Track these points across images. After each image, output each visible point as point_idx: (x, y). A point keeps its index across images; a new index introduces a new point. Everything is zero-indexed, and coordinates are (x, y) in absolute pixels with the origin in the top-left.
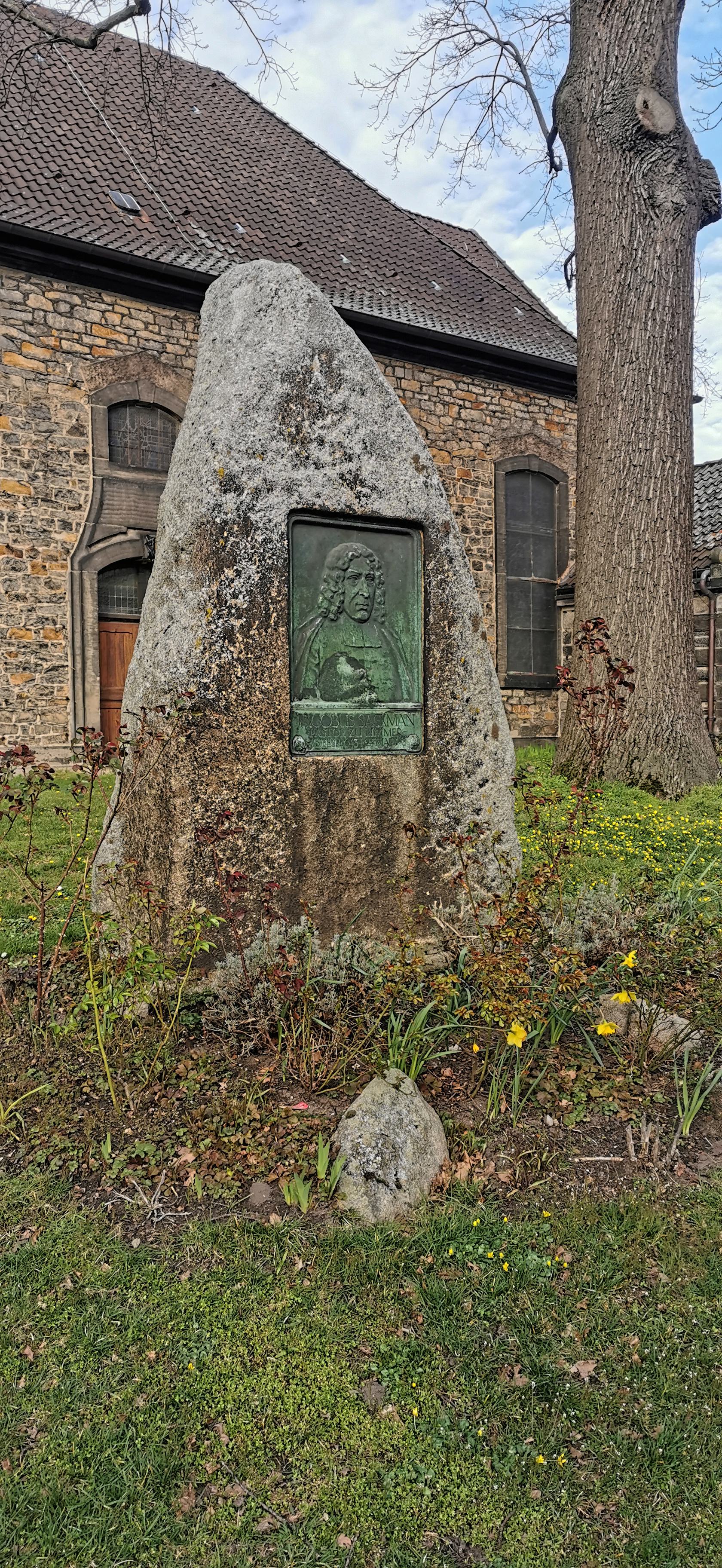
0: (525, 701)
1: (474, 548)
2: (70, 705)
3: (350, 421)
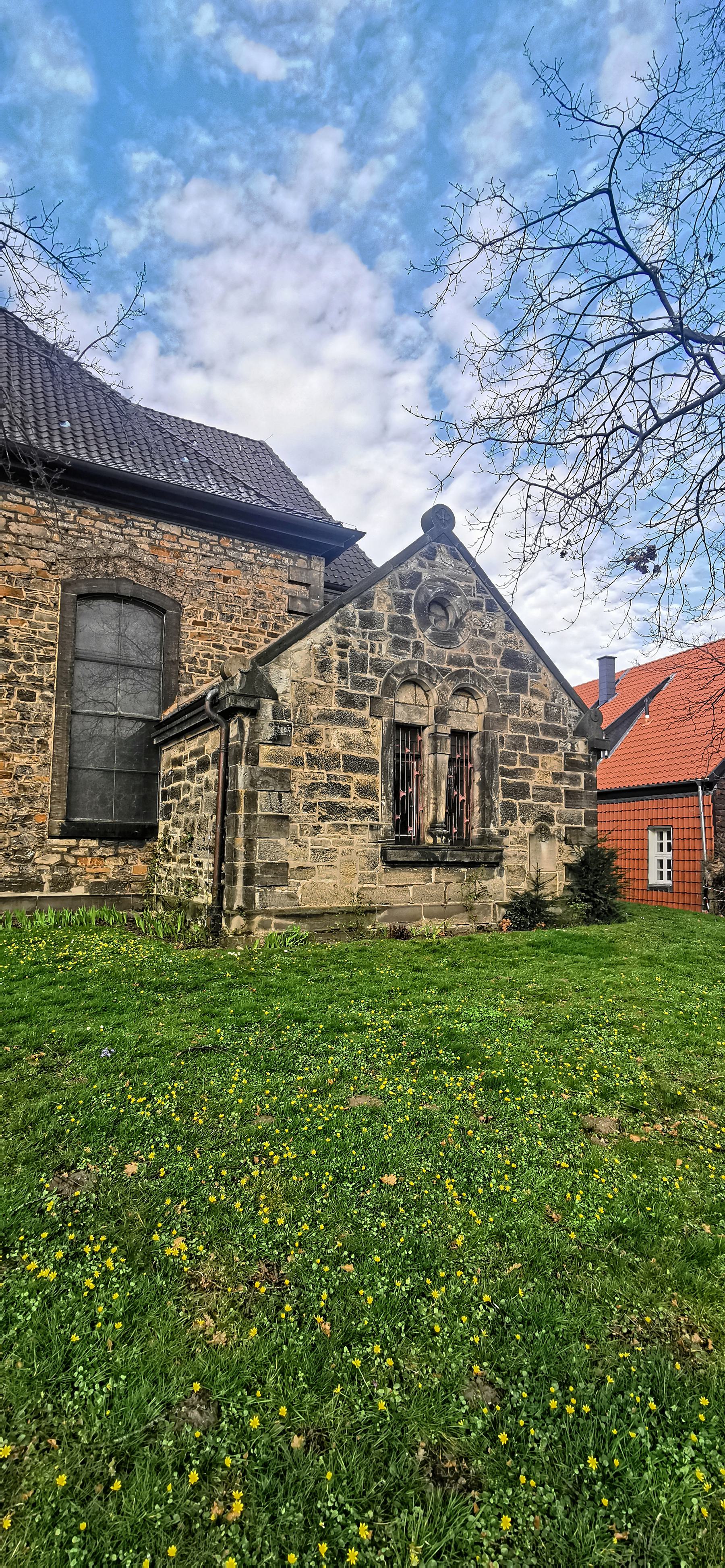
0: (99, 852)
1: (23, 676)
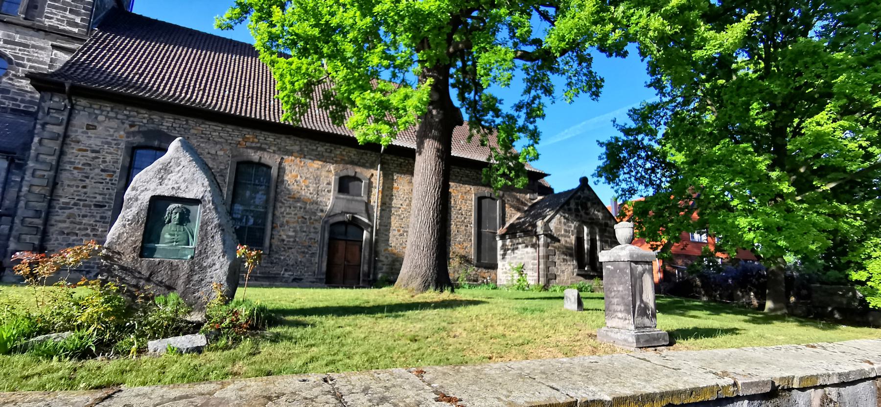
2: (317, 265)
3: (180, 174)
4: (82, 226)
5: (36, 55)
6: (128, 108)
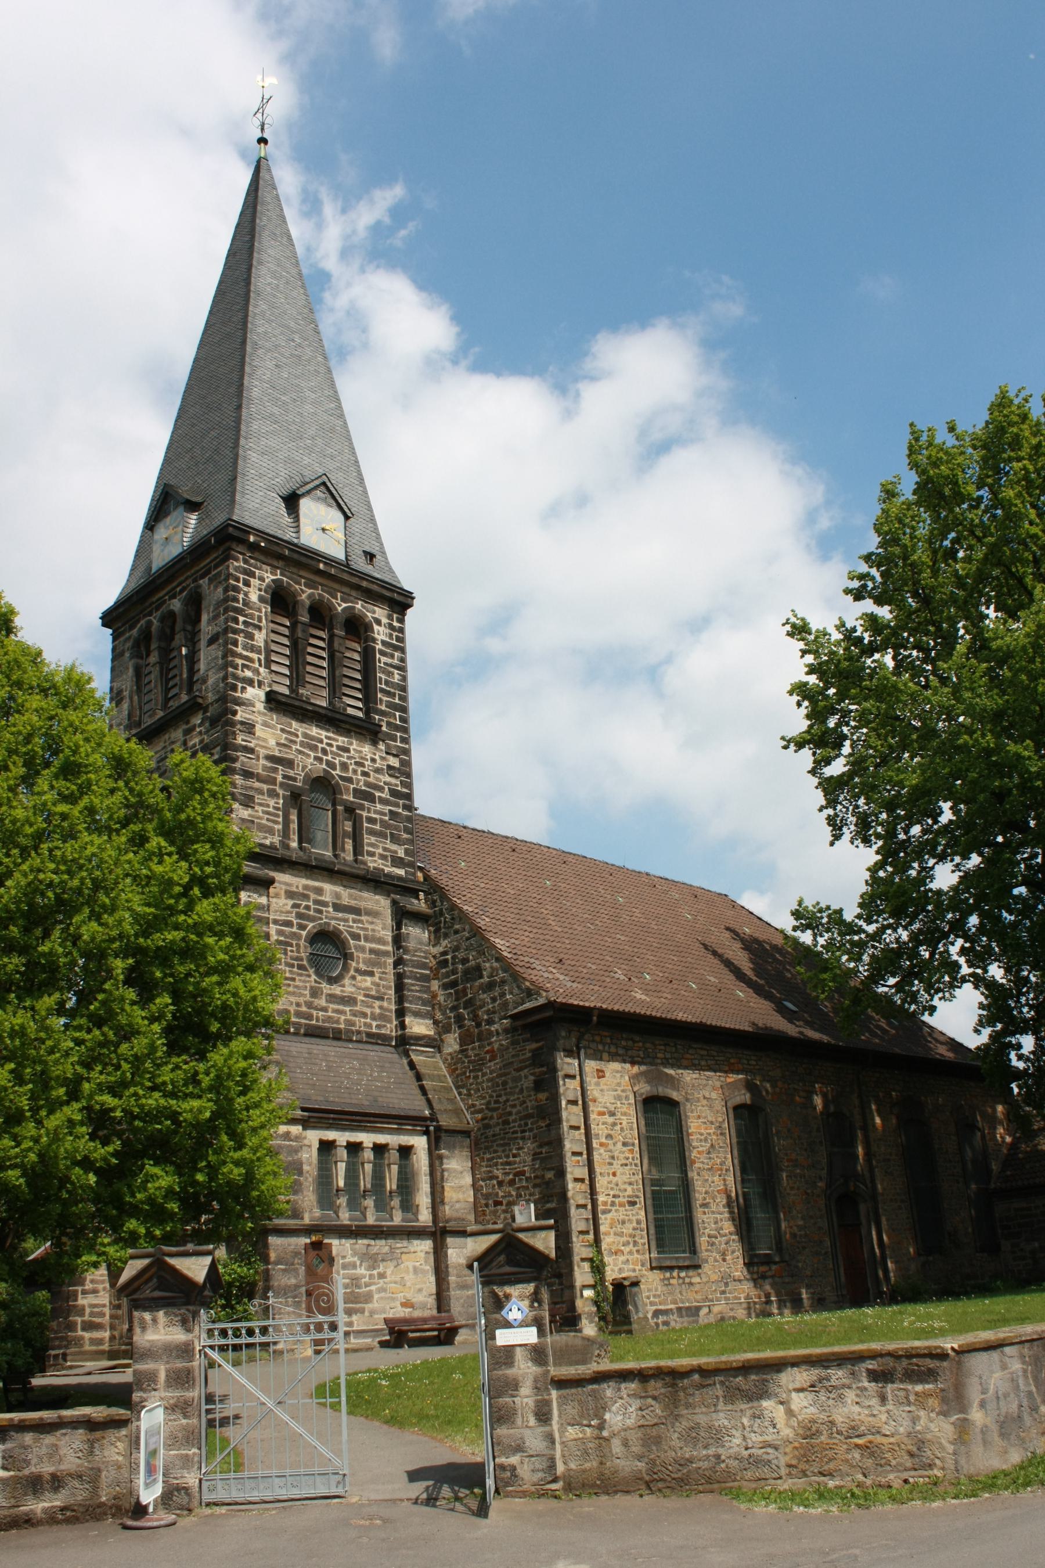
4: (625, 1239)
5: (370, 927)
6: (624, 1036)
